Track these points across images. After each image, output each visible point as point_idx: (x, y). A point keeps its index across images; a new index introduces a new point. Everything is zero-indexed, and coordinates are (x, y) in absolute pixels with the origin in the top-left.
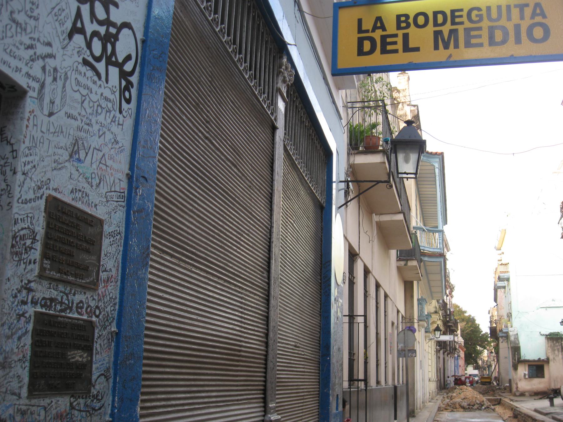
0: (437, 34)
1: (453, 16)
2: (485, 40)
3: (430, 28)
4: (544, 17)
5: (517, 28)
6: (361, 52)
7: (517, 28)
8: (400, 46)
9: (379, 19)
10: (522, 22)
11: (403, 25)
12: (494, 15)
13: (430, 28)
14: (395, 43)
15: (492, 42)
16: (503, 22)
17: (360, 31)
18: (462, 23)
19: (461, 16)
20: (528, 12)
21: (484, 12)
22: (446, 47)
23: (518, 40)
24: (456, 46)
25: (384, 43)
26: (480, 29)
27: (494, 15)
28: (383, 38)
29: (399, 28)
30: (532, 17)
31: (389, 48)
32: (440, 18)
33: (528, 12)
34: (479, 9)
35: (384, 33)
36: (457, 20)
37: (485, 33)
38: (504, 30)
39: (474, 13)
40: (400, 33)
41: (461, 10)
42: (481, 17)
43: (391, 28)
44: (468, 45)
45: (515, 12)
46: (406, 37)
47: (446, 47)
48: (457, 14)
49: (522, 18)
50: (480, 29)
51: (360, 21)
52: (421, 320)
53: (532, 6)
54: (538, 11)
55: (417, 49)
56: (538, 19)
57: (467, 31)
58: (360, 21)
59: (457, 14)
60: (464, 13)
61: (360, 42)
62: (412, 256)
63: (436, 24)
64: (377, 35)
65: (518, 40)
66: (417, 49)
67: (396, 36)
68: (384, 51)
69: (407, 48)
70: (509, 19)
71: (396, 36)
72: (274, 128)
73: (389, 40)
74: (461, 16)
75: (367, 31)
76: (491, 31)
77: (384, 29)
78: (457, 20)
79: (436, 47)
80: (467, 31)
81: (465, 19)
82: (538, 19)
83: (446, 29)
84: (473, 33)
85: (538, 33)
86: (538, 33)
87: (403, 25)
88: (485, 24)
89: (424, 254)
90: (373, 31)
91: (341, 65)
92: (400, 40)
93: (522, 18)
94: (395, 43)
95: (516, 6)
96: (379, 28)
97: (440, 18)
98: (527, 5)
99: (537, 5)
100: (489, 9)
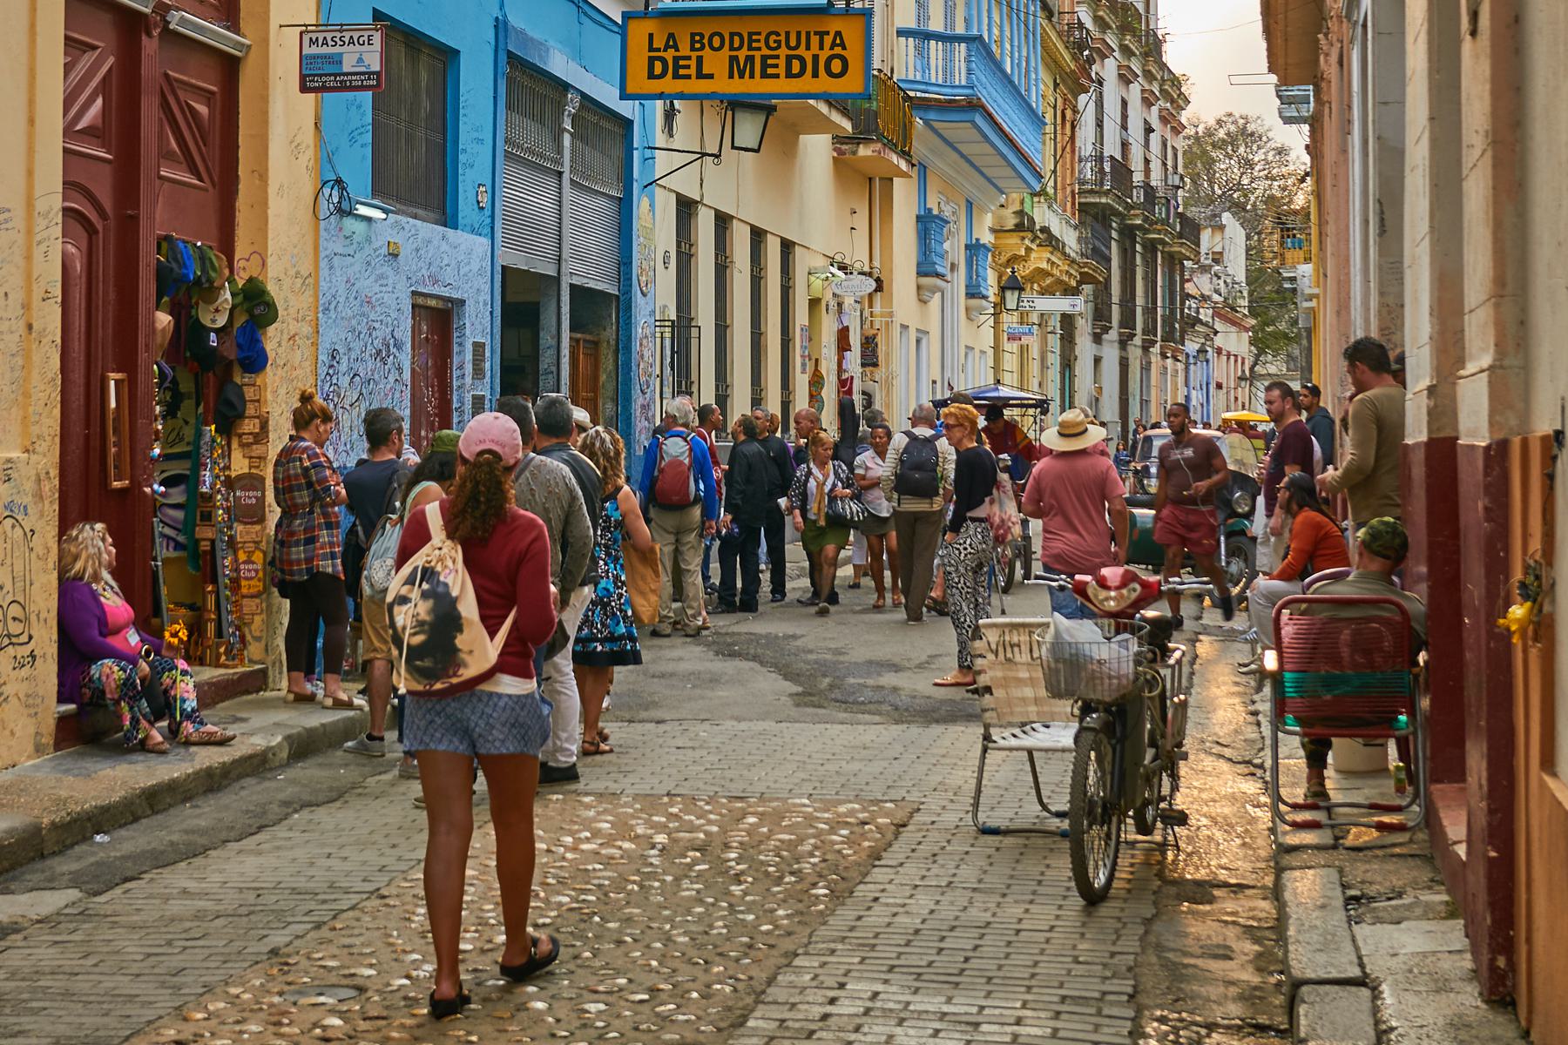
0: (733, 60)
1: (751, 41)
2: (782, 71)
3: (726, 53)
4: (844, 48)
5: (816, 58)
6: (651, 76)
7: (816, 58)
8: (693, 71)
9: (671, 36)
10: (820, 53)
11: (697, 46)
12: (793, 43)
13: (726, 53)
14: (688, 67)
15: (789, 75)
16: (801, 51)
17: (651, 49)
18: (759, 49)
19: (759, 41)
20: (828, 40)
21: (782, 38)
22: (742, 76)
23: (815, 75)
24: (752, 76)
25: (677, 67)
26: (777, 57)
27: (793, 43)
28: (676, 59)
29: (693, 49)
30: (832, 49)
31: (682, 72)
32: (737, 39)
33: (828, 40)
34: (778, 34)
35: (677, 54)
36: (754, 45)
37: (782, 62)
38: (802, 60)
39: (773, 37)
40: (694, 55)
41: (759, 34)
42: (779, 42)
43: (685, 50)
44: (764, 75)
45: (815, 40)
46: (700, 60)
47: (742, 76)
48: (754, 37)
49: (821, 48)
50: (777, 57)
51: (651, 36)
52: (926, 275)
53: (832, 34)
54: (838, 41)
55: (711, 76)
56: (838, 50)
57: (764, 58)
58: (651, 36)
59: (754, 37)
60: (762, 38)
61: (651, 60)
62: (869, 132)
63: (732, 48)
64: (669, 55)
65: (815, 75)
66: (711, 76)
67: (689, 58)
68: (676, 76)
69: (701, 75)
70: (808, 48)
71: (689, 58)
72: (560, 174)
73: (682, 63)
74: (759, 41)
75: (658, 50)
76: (789, 59)
77: (677, 50)
78: (754, 45)
79: (731, 76)
80: (764, 58)
81: (762, 44)
82: (838, 50)
83: (742, 54)
84: (769, 62)
85: (836, 66)
86: (836, 66)
87: (697, 46)
88: (783, 52)
89: (923, 105)
90: (665, 50)
91: (630, 89)
92: (693, 63)
93: (821, 48)
94: (688, 67)
95: (816, 33)
96: (671, 47)
97: (737, 39)
98: (828, 33)
99: (838, 34)
100: (788, 34)
